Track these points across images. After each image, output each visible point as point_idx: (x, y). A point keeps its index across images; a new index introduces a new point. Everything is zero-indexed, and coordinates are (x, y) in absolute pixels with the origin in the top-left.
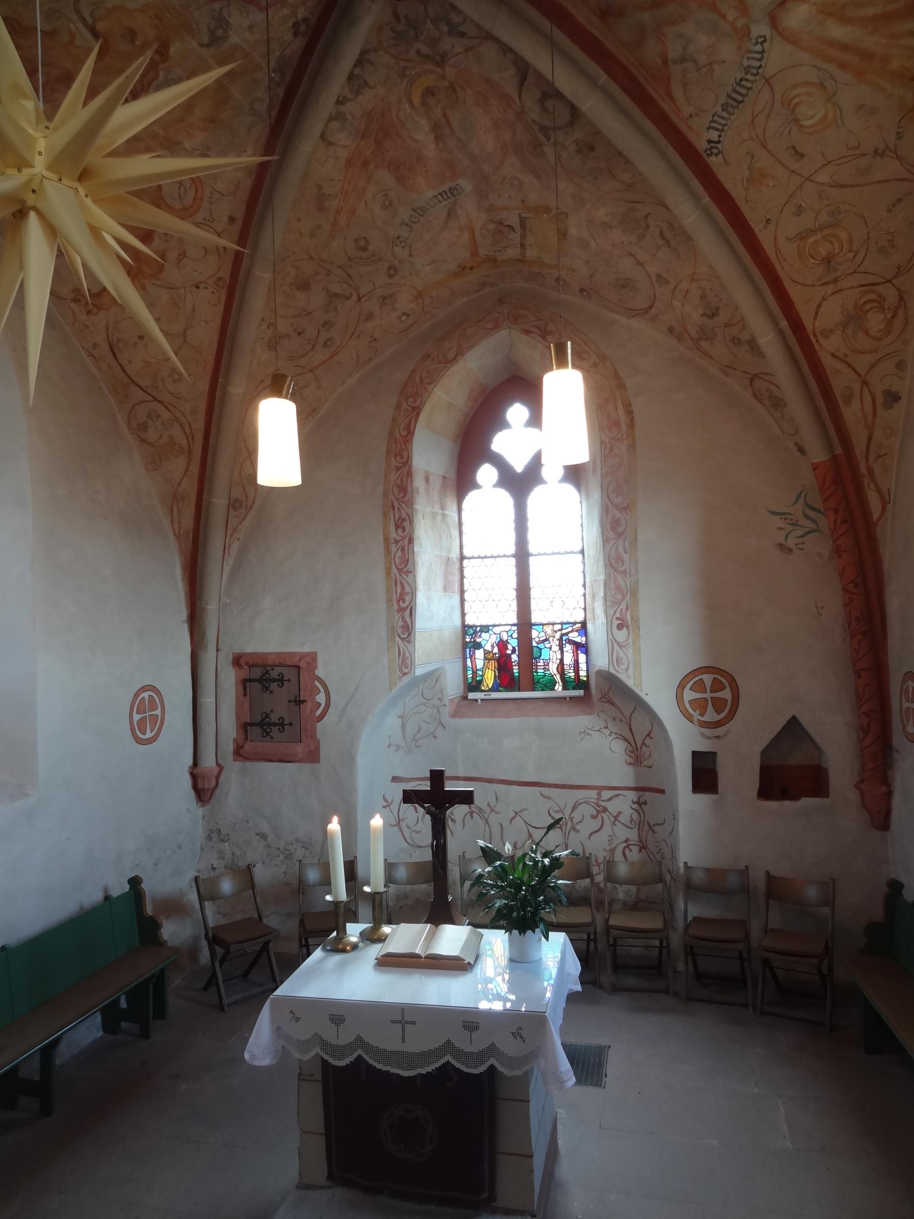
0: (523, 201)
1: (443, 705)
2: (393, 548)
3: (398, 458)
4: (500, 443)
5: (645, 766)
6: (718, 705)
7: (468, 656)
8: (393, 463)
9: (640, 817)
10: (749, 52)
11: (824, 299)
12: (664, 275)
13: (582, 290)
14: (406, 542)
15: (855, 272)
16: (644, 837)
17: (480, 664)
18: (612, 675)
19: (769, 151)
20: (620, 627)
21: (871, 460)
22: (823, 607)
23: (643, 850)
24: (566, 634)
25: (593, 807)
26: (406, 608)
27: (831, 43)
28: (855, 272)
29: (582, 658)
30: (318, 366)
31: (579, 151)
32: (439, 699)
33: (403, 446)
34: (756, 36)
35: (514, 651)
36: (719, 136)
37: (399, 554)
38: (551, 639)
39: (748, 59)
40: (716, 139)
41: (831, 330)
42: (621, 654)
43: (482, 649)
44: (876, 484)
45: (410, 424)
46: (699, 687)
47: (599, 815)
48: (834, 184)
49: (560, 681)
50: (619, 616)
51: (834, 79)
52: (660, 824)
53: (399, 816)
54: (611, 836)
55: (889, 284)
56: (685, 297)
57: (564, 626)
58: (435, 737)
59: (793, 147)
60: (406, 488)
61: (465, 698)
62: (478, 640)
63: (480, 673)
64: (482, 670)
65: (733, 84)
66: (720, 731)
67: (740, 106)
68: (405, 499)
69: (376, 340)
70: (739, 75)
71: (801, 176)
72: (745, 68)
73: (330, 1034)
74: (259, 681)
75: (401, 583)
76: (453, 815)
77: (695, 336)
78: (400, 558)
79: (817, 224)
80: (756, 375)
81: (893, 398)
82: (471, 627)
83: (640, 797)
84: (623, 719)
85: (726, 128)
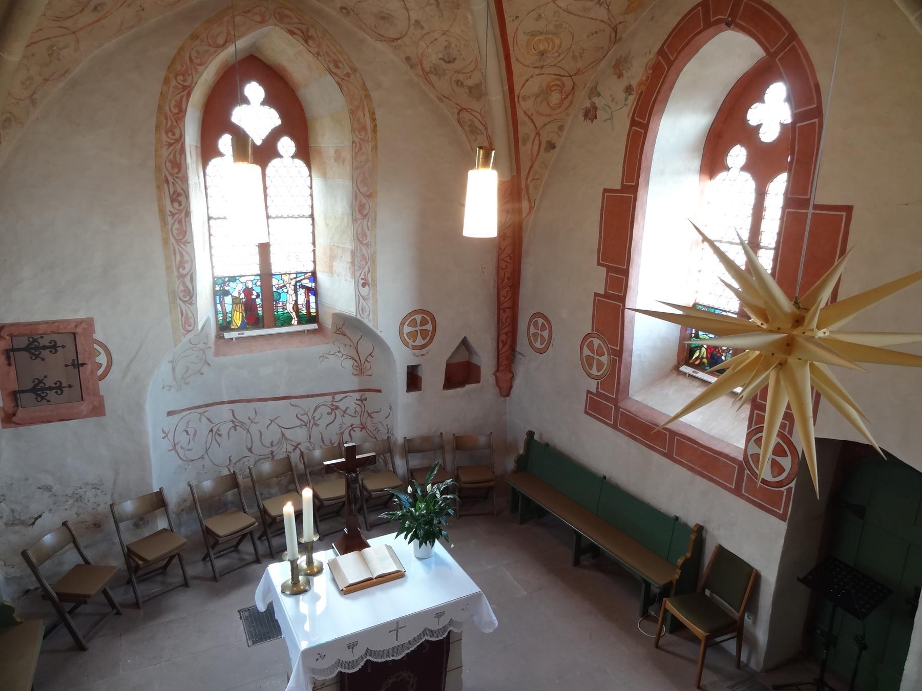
1: (209, 348)
2: (170, 220)
3: (170, 134)
4: (239, 116)
5: (367, 375)
6: (424, 334)
7: (218, 302)
8: (164, 138)
9: (361, 406)
11: (532, 77)
12: (422, 23)
13: (342, 8)
14: (183, 215)
16: (364, 422)
17: (229, 308)
18: (359, 320)
20: (364, 285)
21: (529, 181)
22: (485, 268)
23: (363, 430)
24: (300, 281)
25: (329, 407)
26: (186, 275)
28: (555, 66)
29: (312, 298)
30: (81, 29)
32: (205, 343)
33: (175, 124)
35: (258, 296)
37: (176, 225)
38: (288, 285)
41: (529, 97)
42: (365, 304)
43: (230, 296)
44: (528, 196)
45: (181, 102)
46: (413, 323)
47: (333, 412)
49: (295, 317)
50: (363, 277)
52: (377, 412)
53: (174, 442)
54: (341, 424)
56: (432, 42)
57: (298, 275)
58: (202, 374)
60: (180, 164)
61: (220, 337)
62: (227, 288)
63: (230, 315)
64: (231, 312)
66: (424, 351)
68: (180, 175)
69: (143, 10)
73: (348, 656)
74: (26, 349)
75: (180, 252)
76: (219, 431)
77: (427, 69)
78: (177, 229)
80: (465, 109)
81: (551, 146)
82: (221, 278)
83: (362, 395)
84: (352, 345)
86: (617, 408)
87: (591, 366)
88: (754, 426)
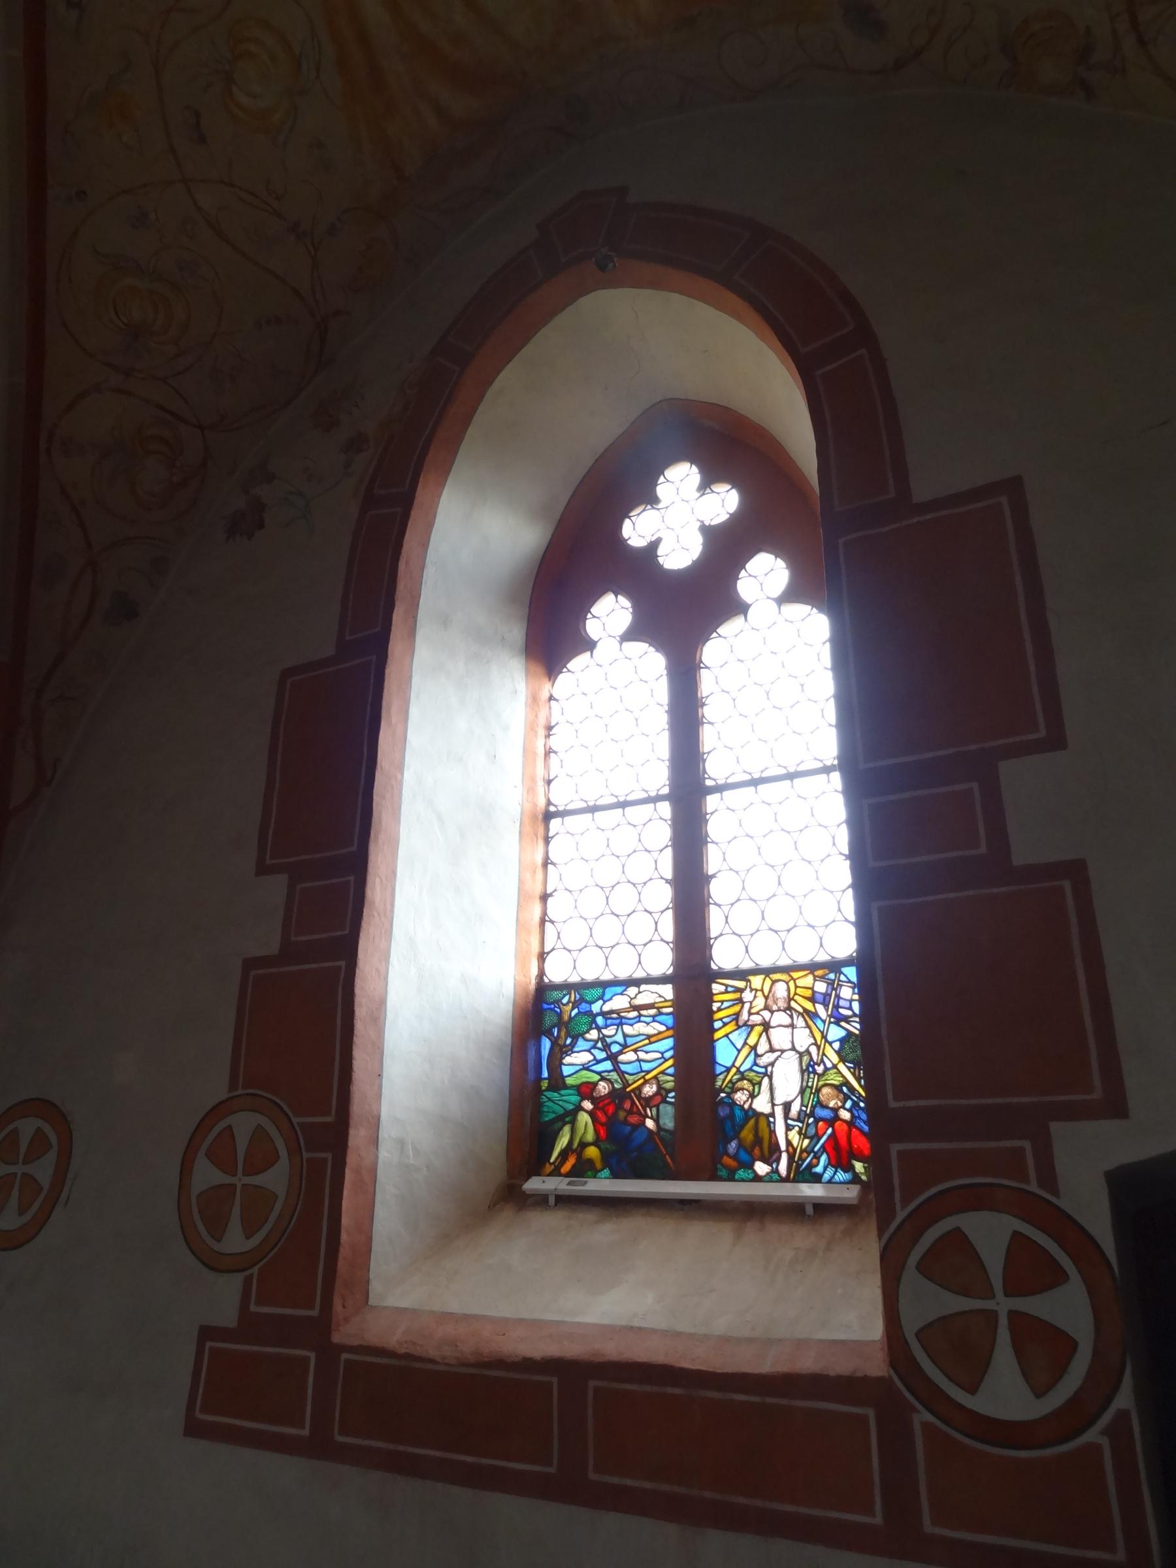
86: (328, 1352)
87: (217, 1227)
88: (903, 1207)
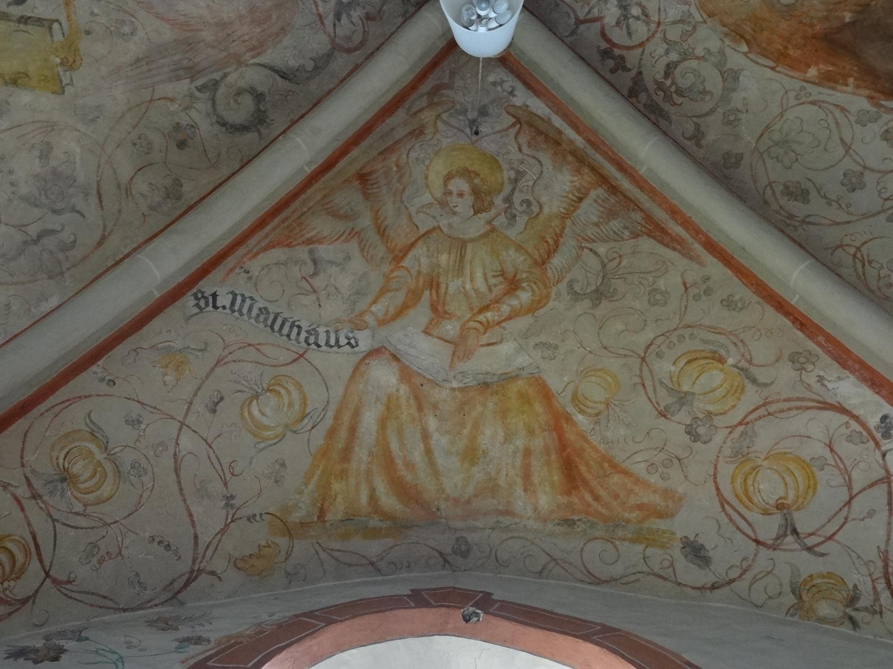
0: (88, 33)
10: (337, 332)
15: (54, 521)
19: (212, 369)
27: (357, 414)
28: (54, 521)
31: (177, 127)
34: (357, 336)
36: (224, 307)
39: (327, 332)
40: (219, 304)
48: (180, 458)
51: (313, 428)
55: (43, 574)
59: (222, 399)
65: (292, 317)
67: (268, 328)
70: (304, 325)
71: (186, 414)
72: (313, 329)
79: (117, 450)
85: (236, 314)
